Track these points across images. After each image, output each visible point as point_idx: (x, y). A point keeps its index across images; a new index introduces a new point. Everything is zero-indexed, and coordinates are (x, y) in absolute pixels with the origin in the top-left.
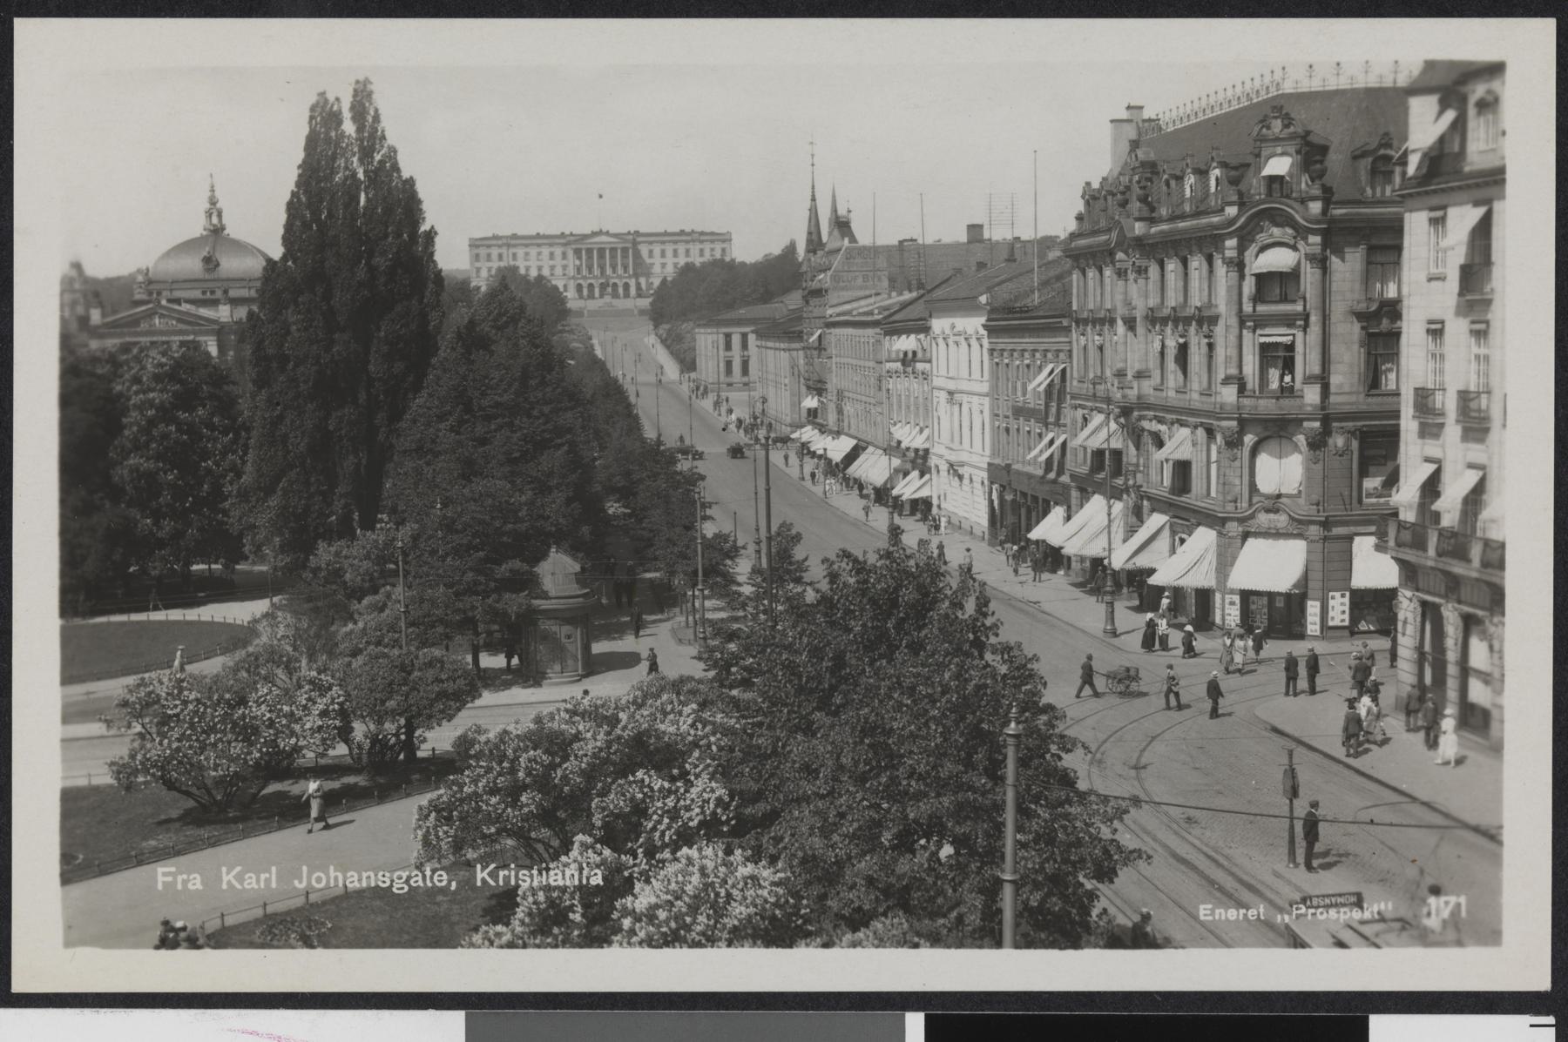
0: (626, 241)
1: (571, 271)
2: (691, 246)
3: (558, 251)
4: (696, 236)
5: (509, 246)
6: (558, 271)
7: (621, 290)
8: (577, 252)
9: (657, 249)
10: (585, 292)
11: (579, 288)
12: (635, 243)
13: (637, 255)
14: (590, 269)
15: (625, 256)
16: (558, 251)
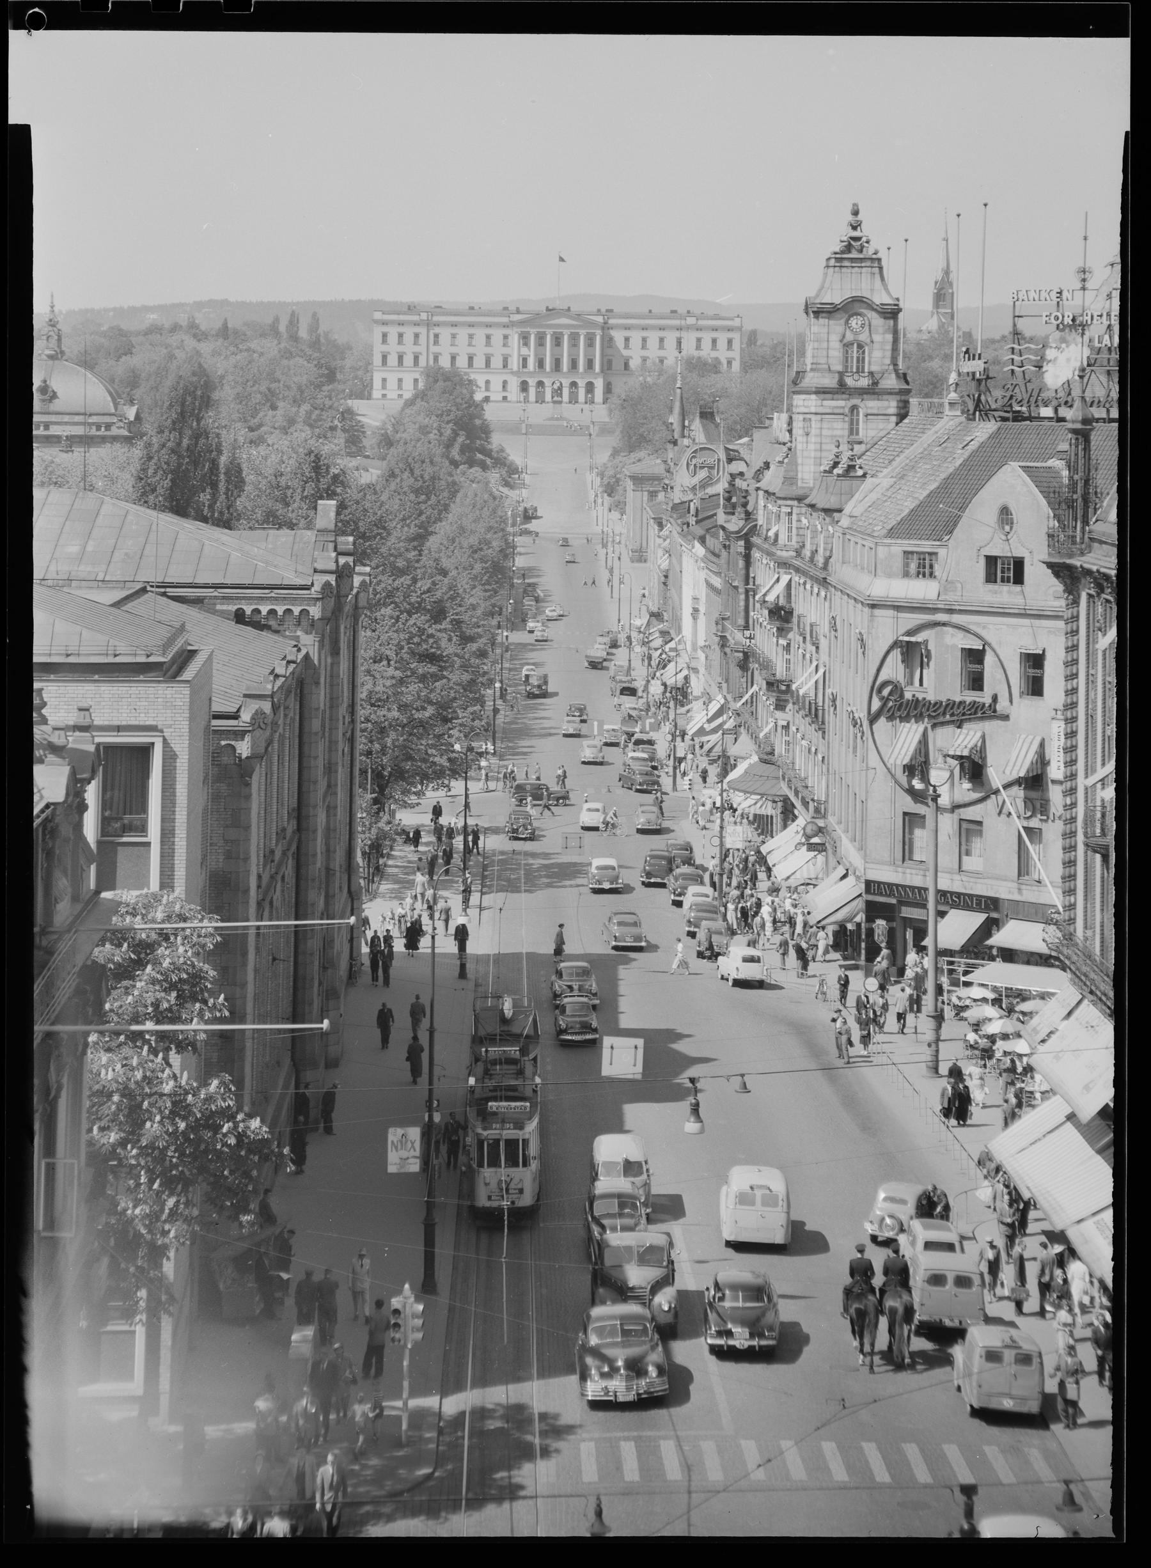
0: (593, 324)
1: (514, 363)
2: (684, 334)
3: (497, 335)
4: (691, 321)
5: (429, 324)
6: (497, 362)
7: (582, 392)
8: (525, 338)
9: (636, 337)
10: (532, 391)
11: (524, 387)
12: (605, 327)
13: (608, 342)
14: (541, 364)
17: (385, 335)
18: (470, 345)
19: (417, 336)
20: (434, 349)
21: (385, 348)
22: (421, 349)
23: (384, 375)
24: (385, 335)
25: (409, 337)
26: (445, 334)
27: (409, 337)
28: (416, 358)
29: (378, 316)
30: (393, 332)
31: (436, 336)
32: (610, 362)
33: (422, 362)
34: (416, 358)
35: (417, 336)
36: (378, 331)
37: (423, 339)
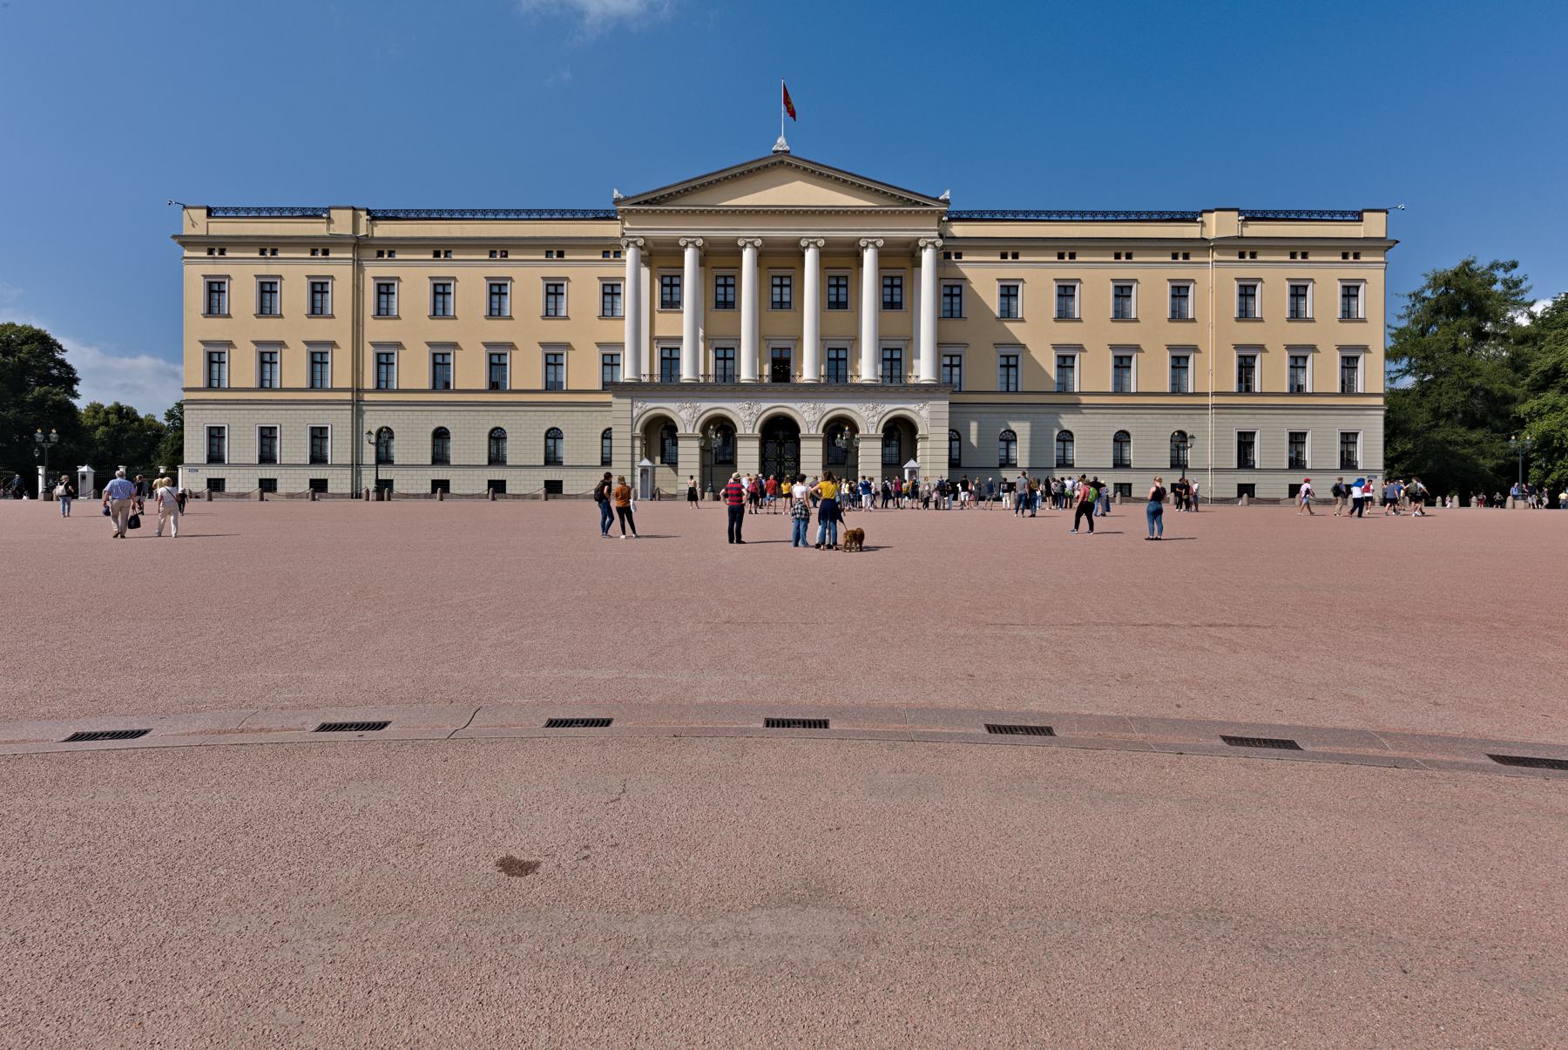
15: (895, 296)
16: (583, 279)
17: (215, 289)
19: (318, 288)
20: (377, 330)
21: (216, 329)
22: (336, 329)
23: (216, 418)
24: (215, 289)
25: (294, 295)
26: (414, 279)
27: (294, 295)
28: (318, 359)
29: (196, 223)
30: (243, 276)
31: (385, 289)
33: (340, 372)
34: (318, 359)
35: (318, 288)
36: (196, 273)
37: (340, 297)
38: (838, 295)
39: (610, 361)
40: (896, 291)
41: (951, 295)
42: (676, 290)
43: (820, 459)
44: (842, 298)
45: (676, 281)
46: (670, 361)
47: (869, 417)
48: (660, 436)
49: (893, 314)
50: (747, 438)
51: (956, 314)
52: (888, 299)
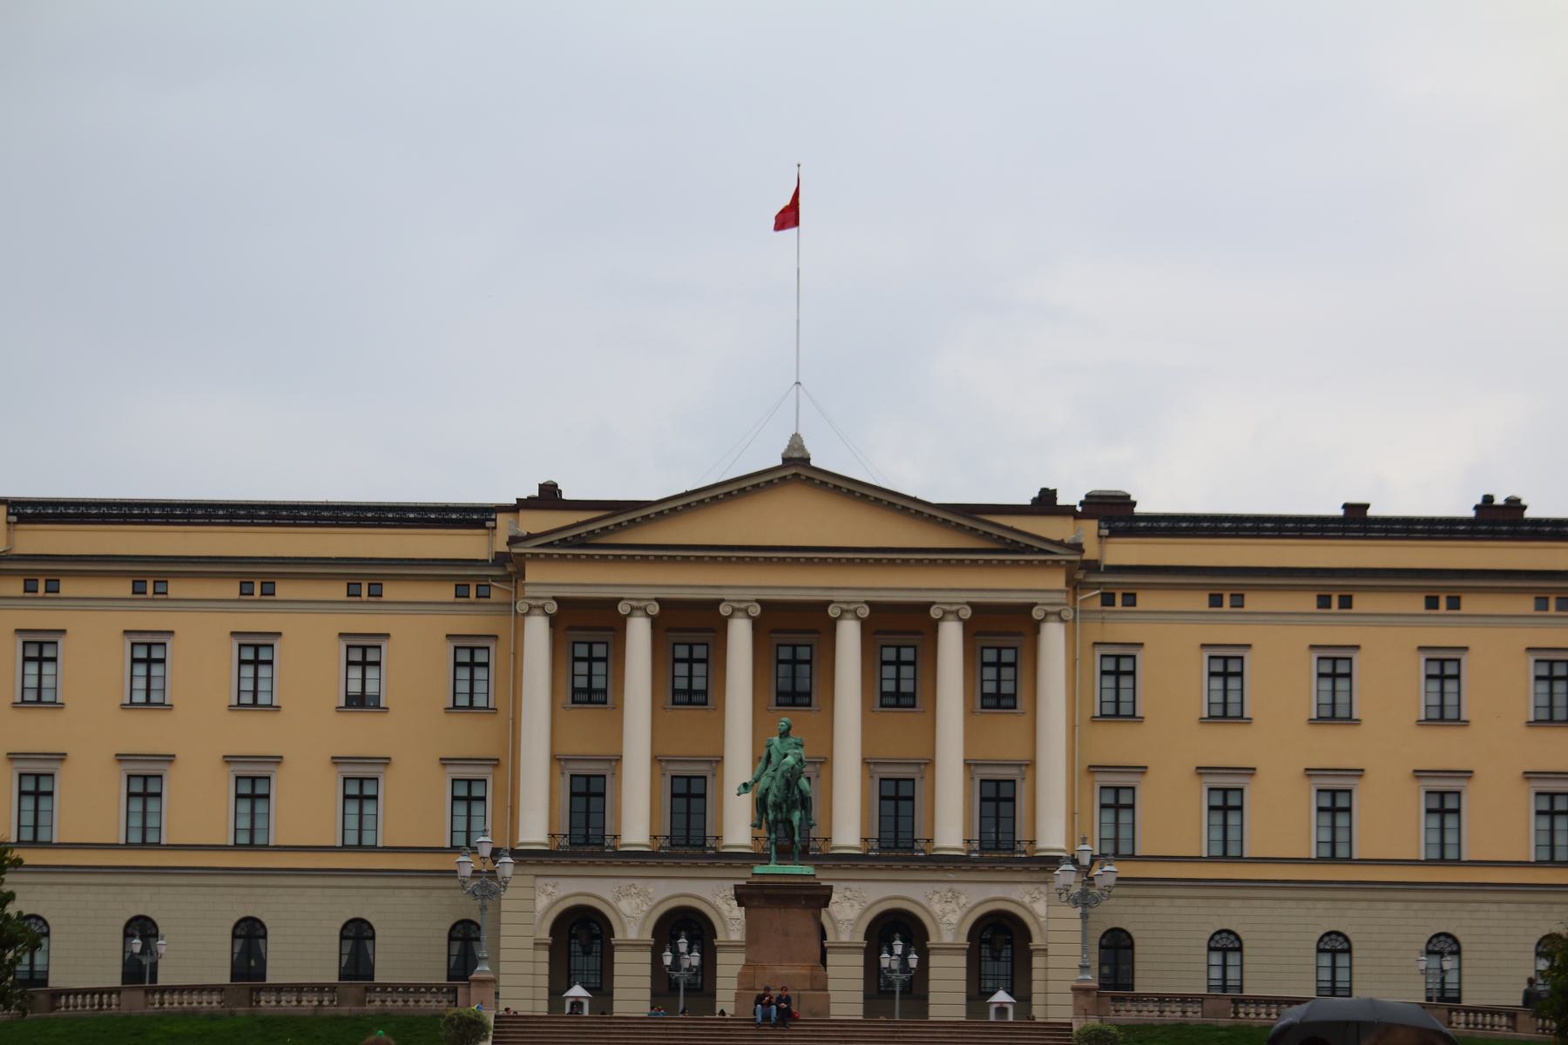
3: (418, 637)
18: (252, 703)
32: (1119, 802)
38: (900, 691)
39: (467, 796)
40: (1007, 673)
41: (1117, 673)
42: (598, 668)
43: (860, 985)
44: (906, 686)
45: (599, 651)
46: (587, 794)
47: (949, 910)
48: (581, 937)
49: (1002, 722)
50: (732, 947)
51: (1125, 709)
52: (990, 688)
